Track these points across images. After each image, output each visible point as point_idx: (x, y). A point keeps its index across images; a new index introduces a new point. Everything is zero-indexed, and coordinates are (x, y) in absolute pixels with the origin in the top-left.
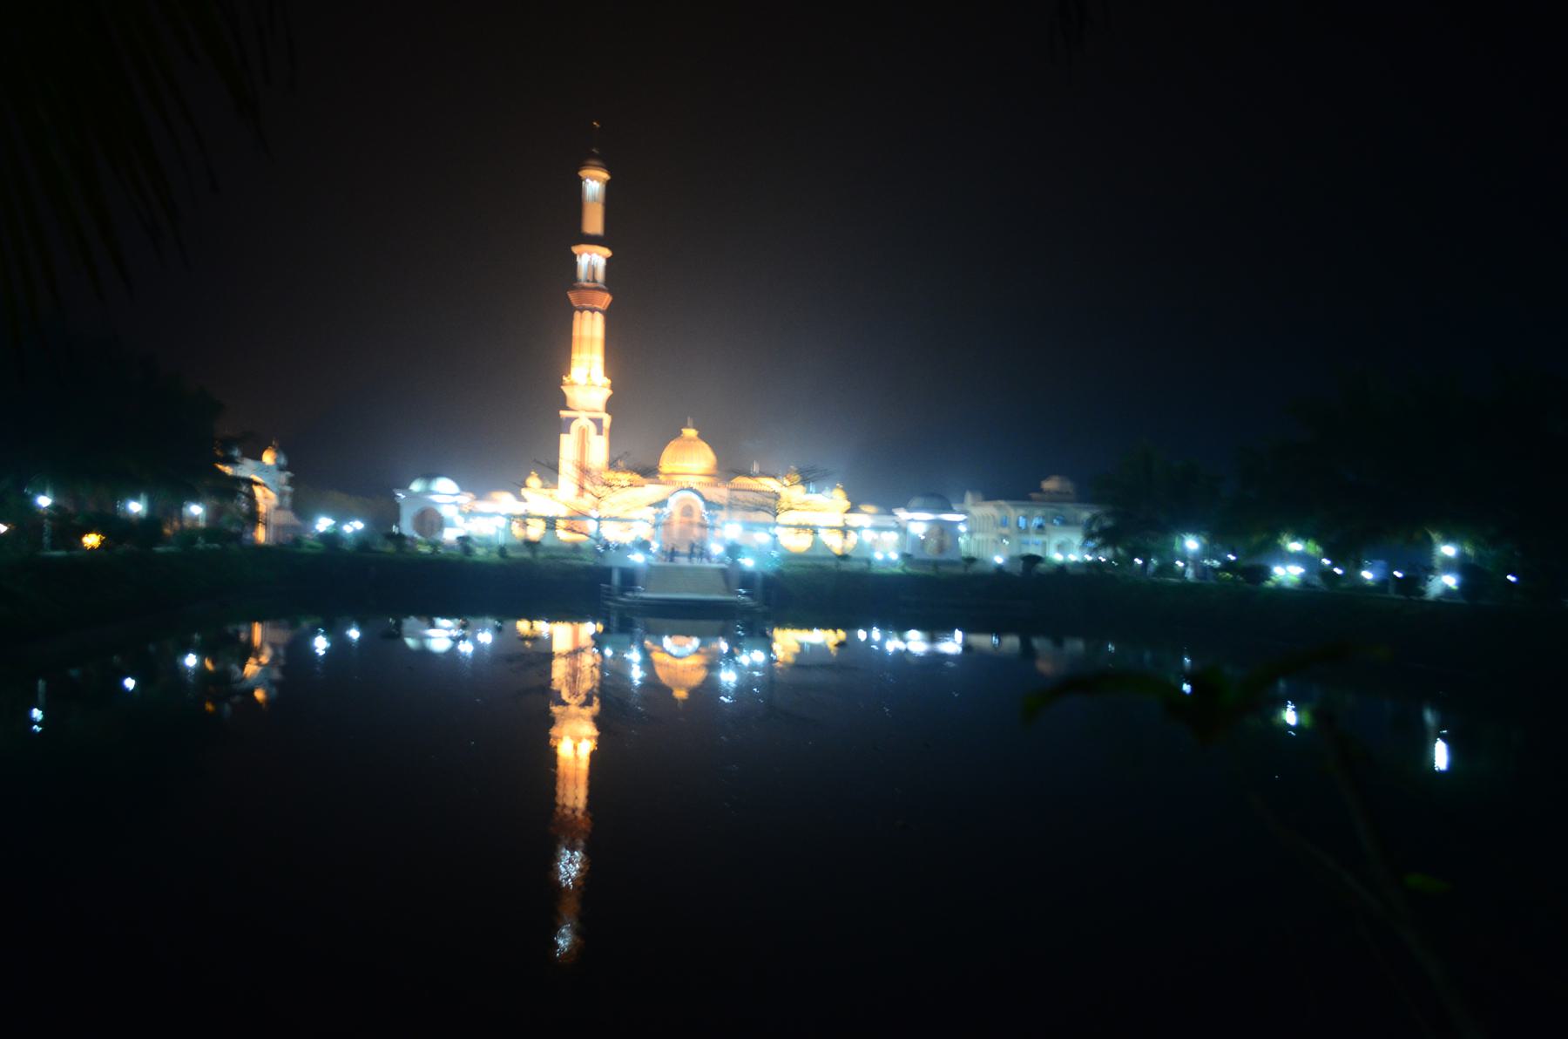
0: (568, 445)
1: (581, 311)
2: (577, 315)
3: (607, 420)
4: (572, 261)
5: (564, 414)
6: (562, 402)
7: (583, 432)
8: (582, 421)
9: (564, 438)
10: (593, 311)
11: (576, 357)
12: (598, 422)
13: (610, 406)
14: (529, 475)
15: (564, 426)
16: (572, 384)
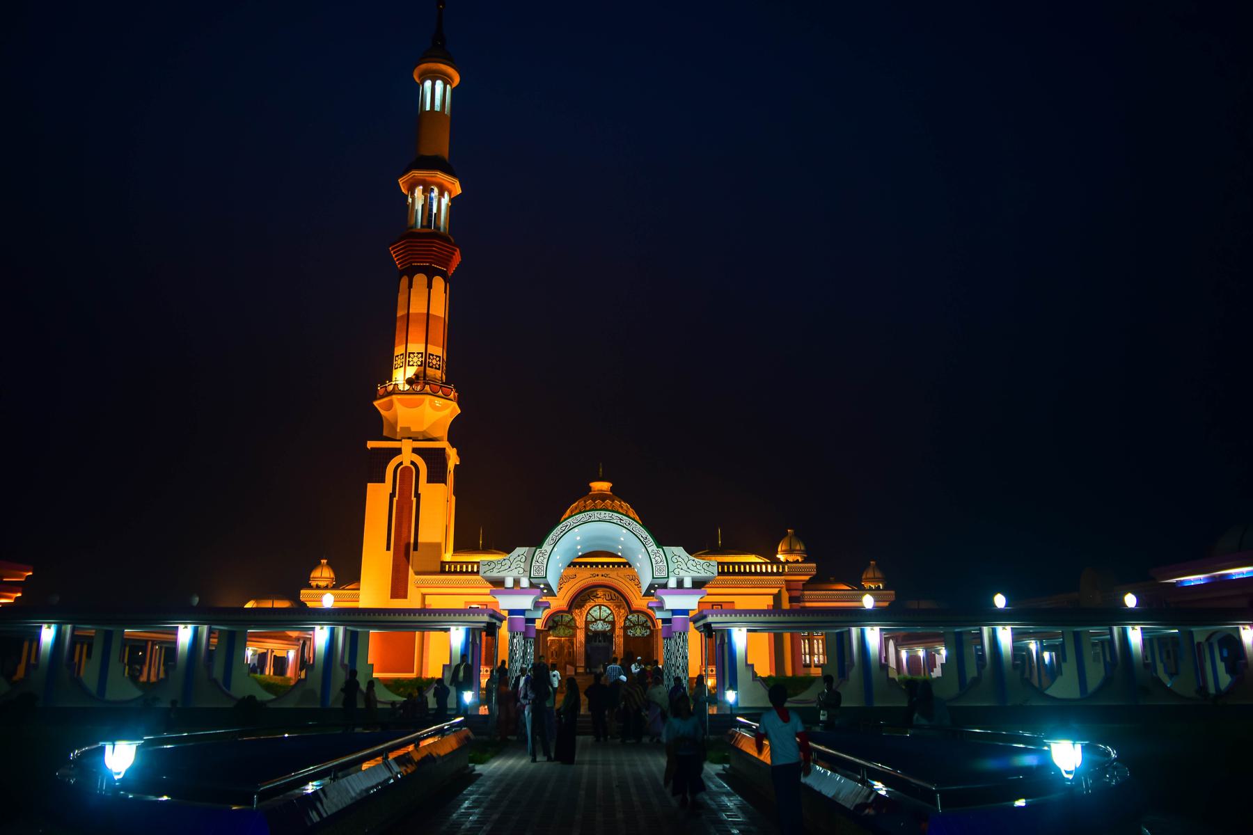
0: (378, 497)
1: (411, 272)
2: (404, 281)
3: (453, 459)
4: (403, 207)
5: (371, 444)
6: (376, 426)
7: (406, 477)
8: (407, 457)
9: (371, 487)
10: (430, 274)
11: (399, 350)
12: (435, 460)
13: (457, 432)
14: (316, 564)
15: (375, 466)
16: (395, 392)
